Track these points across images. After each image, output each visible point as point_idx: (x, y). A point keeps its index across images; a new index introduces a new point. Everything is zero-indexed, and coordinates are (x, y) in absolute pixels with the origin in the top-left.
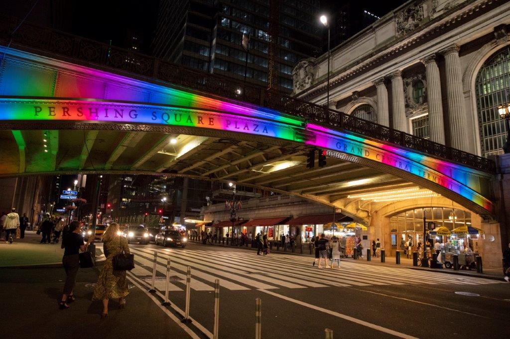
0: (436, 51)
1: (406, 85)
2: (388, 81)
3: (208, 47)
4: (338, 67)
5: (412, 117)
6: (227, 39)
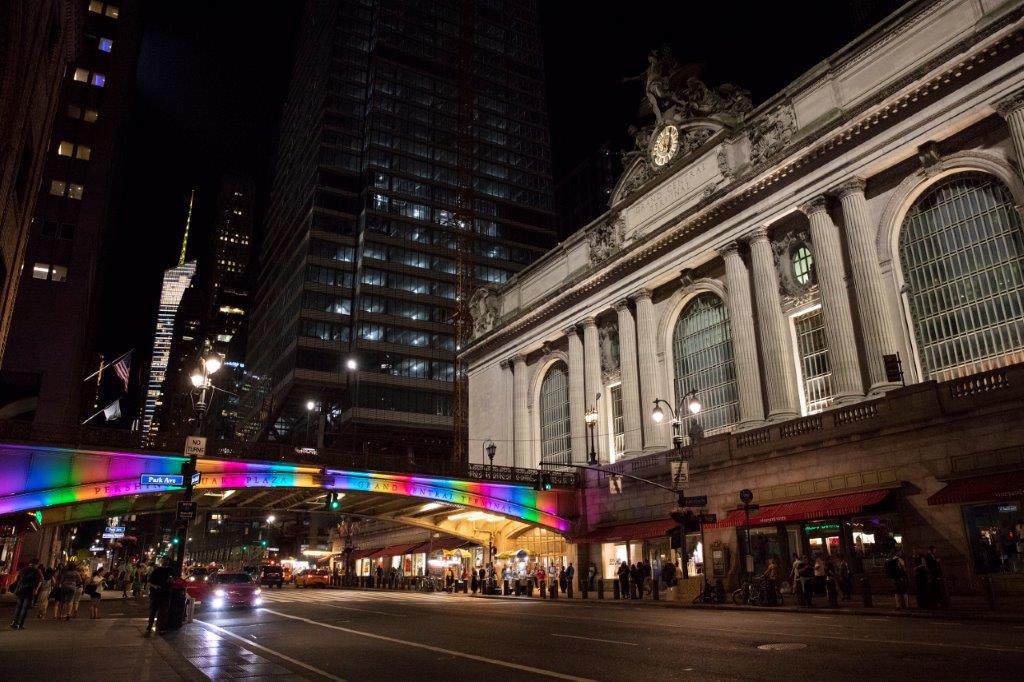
0: (626, 295)
1: (602, 337)
2: (580, 330)
3: (353, 247)
4: (528, 300)
5: (609, 384)
6: (385, 230)
